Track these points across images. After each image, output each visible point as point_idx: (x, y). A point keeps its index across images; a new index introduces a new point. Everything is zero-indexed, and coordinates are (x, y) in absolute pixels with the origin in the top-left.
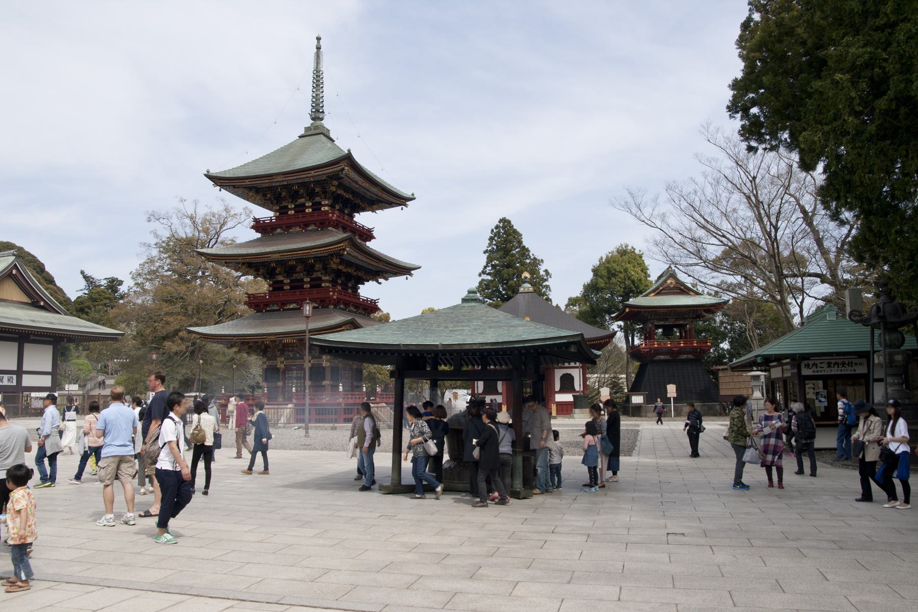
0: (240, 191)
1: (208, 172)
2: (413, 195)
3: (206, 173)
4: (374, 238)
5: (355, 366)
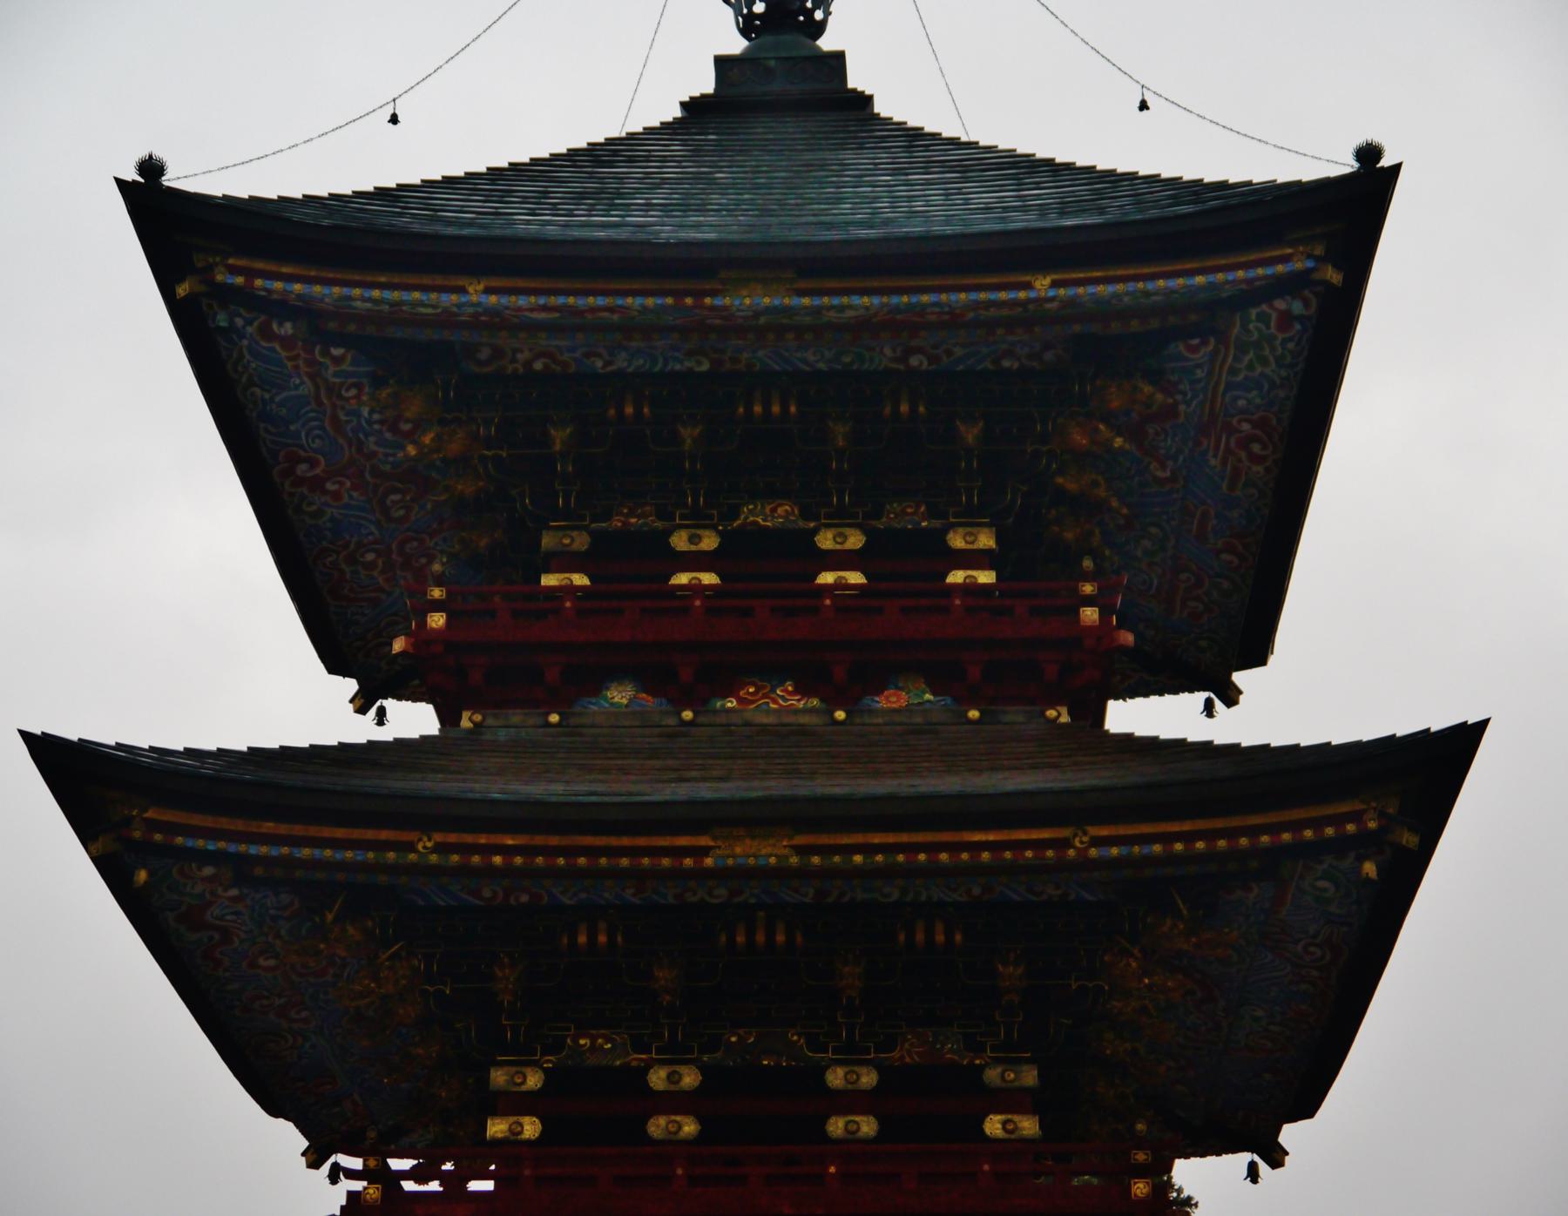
2: (1369, 154)
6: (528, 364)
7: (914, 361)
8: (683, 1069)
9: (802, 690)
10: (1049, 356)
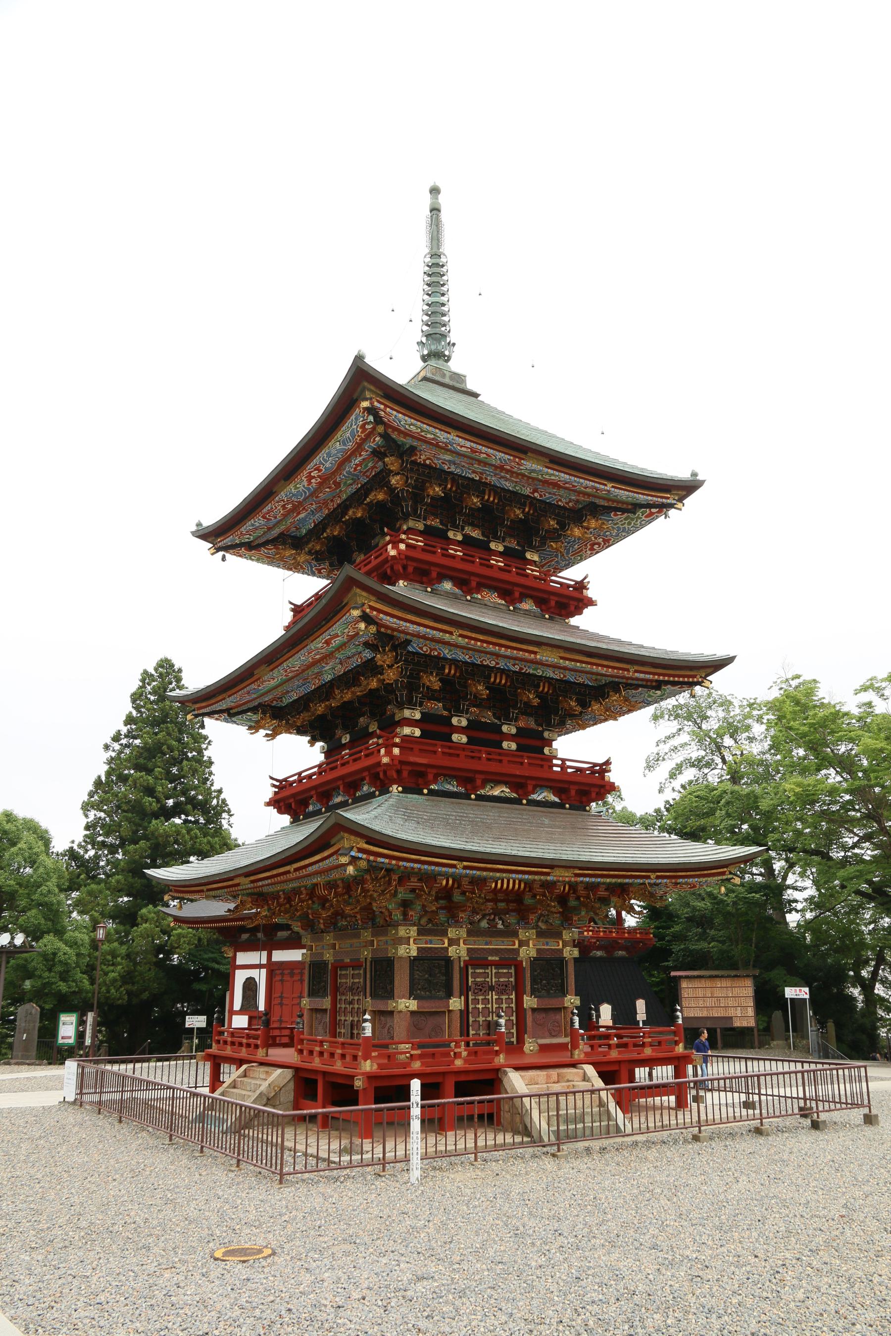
0: (271, 550)
1: (199, 524)
2: (694, 474)
3: (194, 528)
4: (591, 602)
5: (528, 952)
6: (424, 461)
7: (536, 495)
8: (462, 719)
9: (499, 597)
10: (571, 504)
